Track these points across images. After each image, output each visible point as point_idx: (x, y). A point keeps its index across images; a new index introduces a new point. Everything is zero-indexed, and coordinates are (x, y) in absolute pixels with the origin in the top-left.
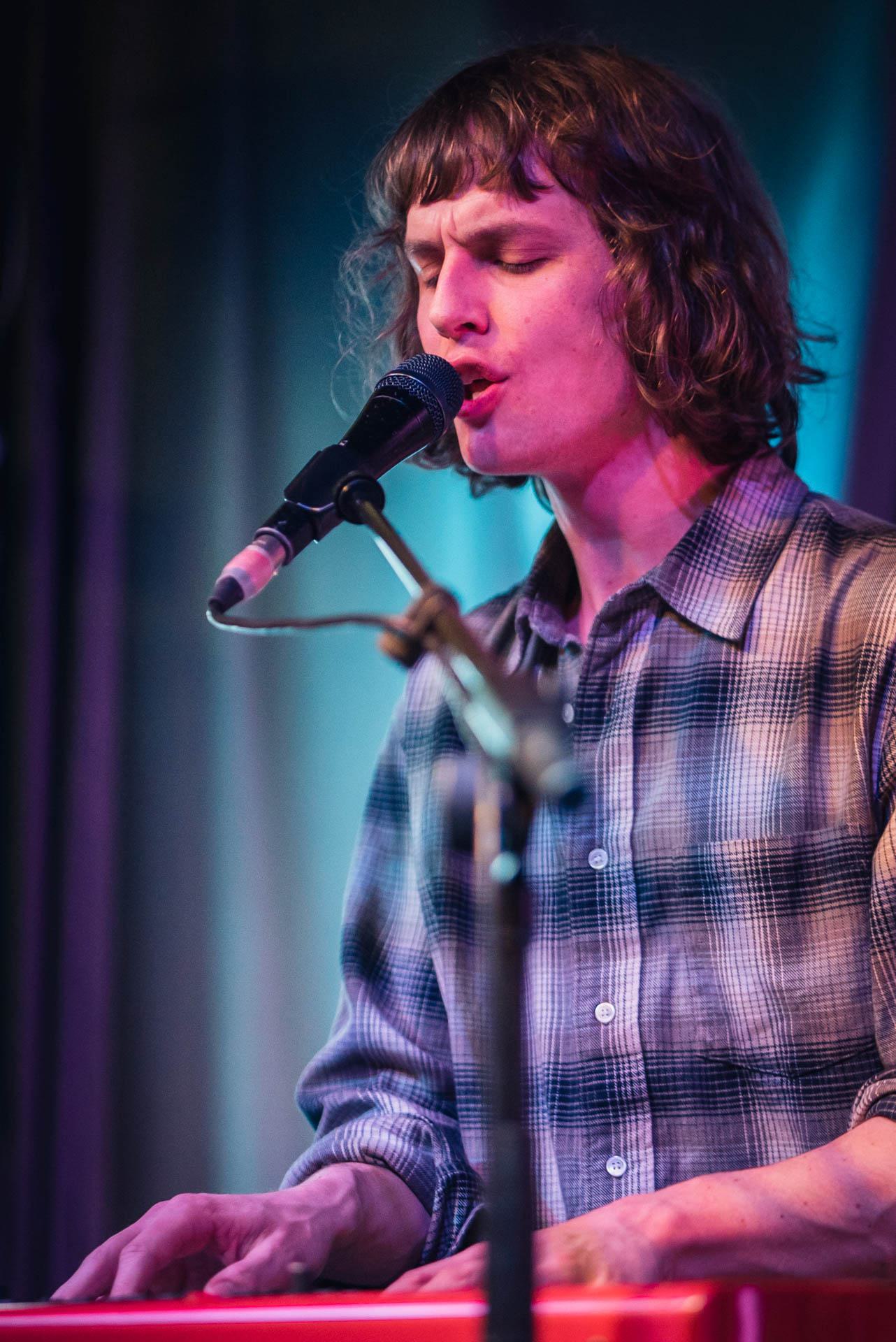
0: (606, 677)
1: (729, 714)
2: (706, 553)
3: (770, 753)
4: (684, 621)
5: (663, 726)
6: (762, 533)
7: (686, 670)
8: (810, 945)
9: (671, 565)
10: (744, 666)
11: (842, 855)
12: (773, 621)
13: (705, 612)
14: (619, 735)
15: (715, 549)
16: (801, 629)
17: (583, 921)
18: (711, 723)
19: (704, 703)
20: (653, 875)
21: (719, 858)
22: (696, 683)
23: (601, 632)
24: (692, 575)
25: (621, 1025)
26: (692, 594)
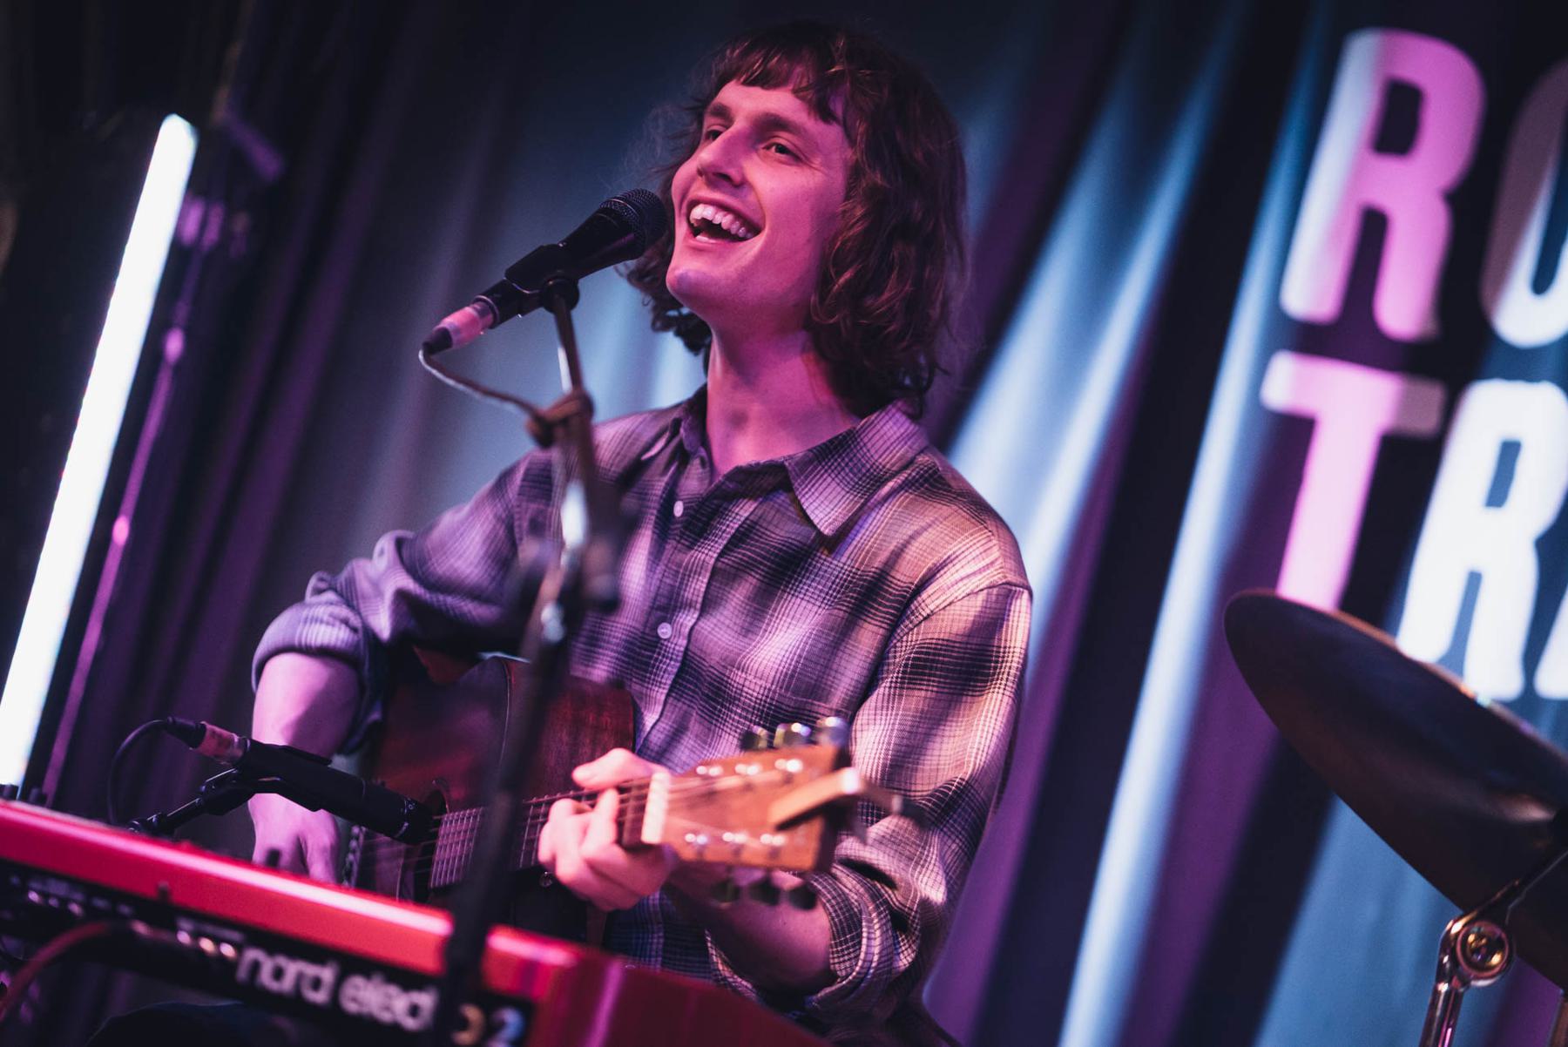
2: (836, 460)
6: (880, 464)
15: (843, 459)
26: (813, 486)
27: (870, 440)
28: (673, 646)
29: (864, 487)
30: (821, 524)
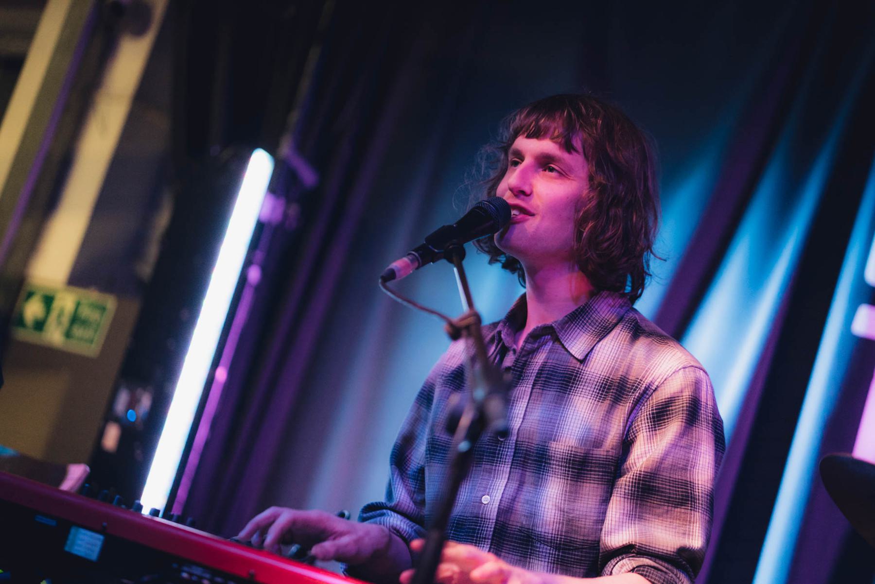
0: (526, 361)
1: (574, 390)
2: (581, 320)
3: (586, 411)
4: (564, 347)
8: (581, 496)
10: (585, 372)
11: (604, 462)
12: (602, 357)
14: (526, 387)
16: (613, 363)
17: (488, 459)
18: (565, 392)
19: (565, 383)
20: (525, 448)
21: (554, 449)
23: (529, 341)
24: (572, 327)
25: (491, 506)
29: (598, 332)
30: (576, 354)
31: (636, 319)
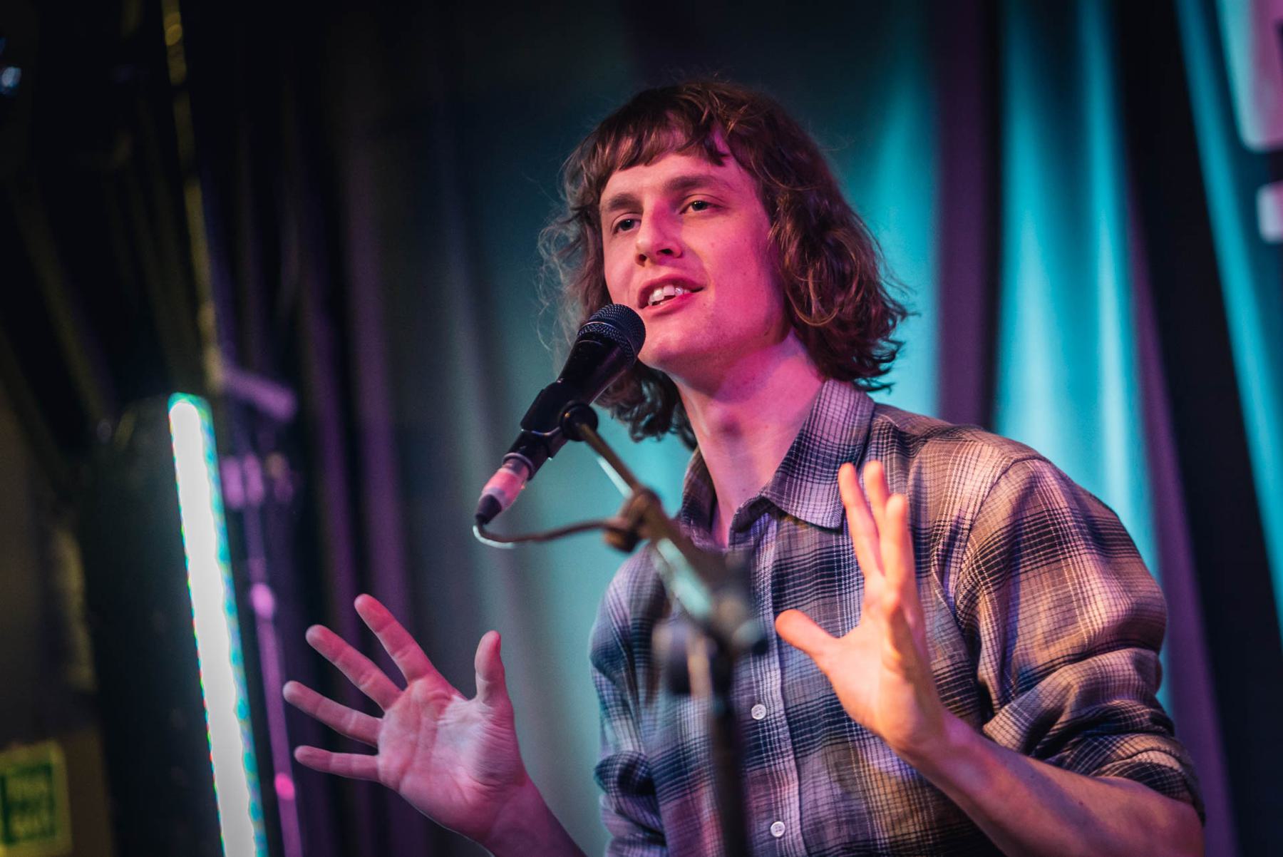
1: (845, 584)
2: (804, 466)
4: (797, 520)
5: (796, 602)
6: (844, 445)
7: (807, 556)
9: (778, 480)
13: (810, 510)
15: (810, 462)
18: (833, 594)
22: (816, 565)
23: (737, 540)
24: (796, 484)
26: (799, 498)
27: (823, 431)
28: (772, 716)
30: (825, 522)
31: (891, 425)
